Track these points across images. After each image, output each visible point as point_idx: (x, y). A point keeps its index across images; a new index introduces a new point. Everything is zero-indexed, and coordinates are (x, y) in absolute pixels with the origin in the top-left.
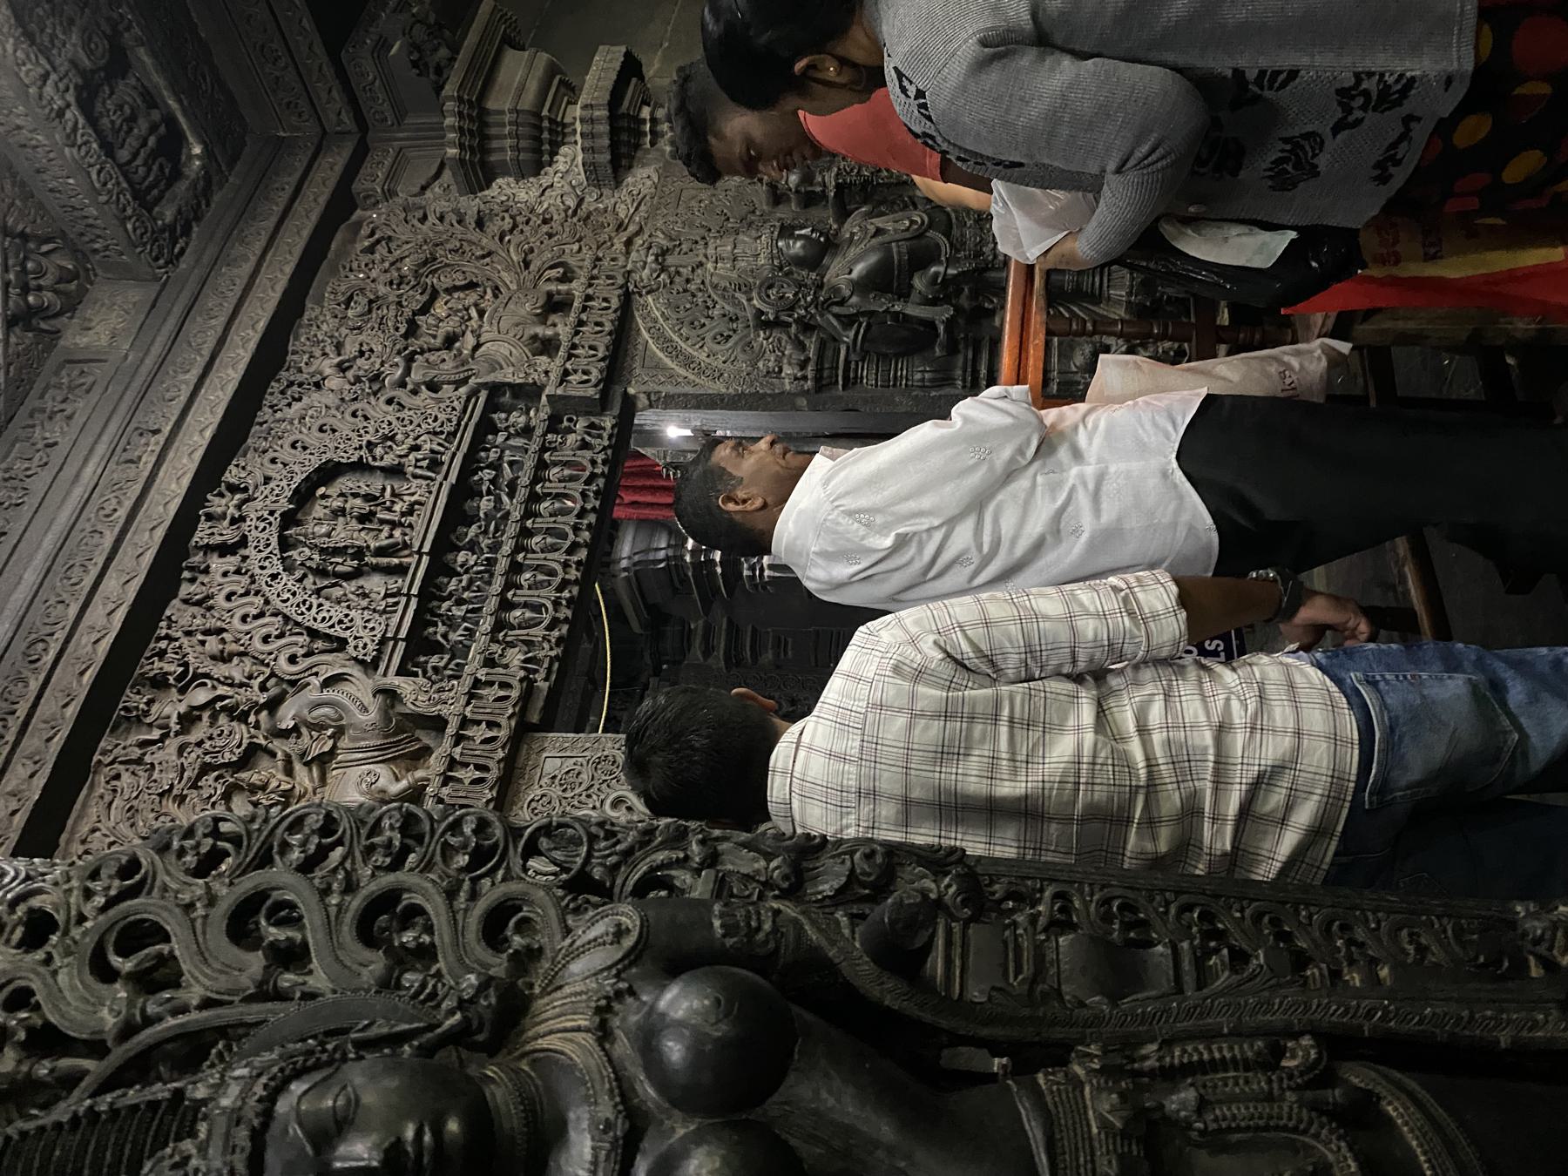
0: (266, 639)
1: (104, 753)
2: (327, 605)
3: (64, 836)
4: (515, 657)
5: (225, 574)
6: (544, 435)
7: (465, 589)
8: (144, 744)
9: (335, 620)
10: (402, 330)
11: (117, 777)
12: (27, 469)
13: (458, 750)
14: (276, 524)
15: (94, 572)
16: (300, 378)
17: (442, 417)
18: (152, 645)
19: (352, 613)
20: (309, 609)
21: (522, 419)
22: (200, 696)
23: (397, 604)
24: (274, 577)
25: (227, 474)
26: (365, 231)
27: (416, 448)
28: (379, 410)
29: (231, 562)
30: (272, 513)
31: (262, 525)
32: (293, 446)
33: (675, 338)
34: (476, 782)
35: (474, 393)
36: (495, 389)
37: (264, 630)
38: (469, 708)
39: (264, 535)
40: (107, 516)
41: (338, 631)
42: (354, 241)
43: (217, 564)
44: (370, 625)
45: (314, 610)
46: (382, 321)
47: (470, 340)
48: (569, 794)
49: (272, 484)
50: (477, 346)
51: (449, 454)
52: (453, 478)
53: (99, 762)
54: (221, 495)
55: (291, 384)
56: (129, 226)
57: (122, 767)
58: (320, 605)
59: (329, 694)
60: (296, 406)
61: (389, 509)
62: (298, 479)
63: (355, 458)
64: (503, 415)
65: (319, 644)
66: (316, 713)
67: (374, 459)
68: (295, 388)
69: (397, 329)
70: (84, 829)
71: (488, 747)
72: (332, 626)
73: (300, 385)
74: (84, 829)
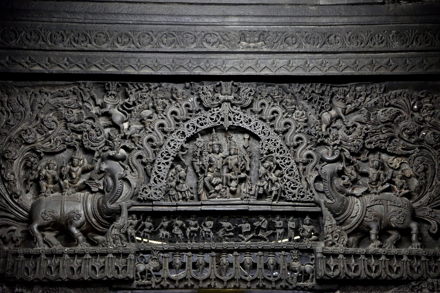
0: (150, 140)
1: (85, 84)
2: (168, 167)
3: (41, 83)
9: (159, 173)
10: (369, 146)
14: (216, 124)
15: (169, 49)
18: (144, 84)
19: (164, 181)
20: (165, 159)
23: (174, 199)
29: (196, 106)
30: (223, 120)
31: (214, 117)
32: (274, 112)
35: (318, 204)
39: (208, 120)
41: (153, 176)
43: (192, 99)
44: (158, 192)
50: (358, 197)
51: (270, 203)
53: (79, 84)
58: (167, 163)
62: (246, 126)
70: (46, 90)
72: (156, 173)
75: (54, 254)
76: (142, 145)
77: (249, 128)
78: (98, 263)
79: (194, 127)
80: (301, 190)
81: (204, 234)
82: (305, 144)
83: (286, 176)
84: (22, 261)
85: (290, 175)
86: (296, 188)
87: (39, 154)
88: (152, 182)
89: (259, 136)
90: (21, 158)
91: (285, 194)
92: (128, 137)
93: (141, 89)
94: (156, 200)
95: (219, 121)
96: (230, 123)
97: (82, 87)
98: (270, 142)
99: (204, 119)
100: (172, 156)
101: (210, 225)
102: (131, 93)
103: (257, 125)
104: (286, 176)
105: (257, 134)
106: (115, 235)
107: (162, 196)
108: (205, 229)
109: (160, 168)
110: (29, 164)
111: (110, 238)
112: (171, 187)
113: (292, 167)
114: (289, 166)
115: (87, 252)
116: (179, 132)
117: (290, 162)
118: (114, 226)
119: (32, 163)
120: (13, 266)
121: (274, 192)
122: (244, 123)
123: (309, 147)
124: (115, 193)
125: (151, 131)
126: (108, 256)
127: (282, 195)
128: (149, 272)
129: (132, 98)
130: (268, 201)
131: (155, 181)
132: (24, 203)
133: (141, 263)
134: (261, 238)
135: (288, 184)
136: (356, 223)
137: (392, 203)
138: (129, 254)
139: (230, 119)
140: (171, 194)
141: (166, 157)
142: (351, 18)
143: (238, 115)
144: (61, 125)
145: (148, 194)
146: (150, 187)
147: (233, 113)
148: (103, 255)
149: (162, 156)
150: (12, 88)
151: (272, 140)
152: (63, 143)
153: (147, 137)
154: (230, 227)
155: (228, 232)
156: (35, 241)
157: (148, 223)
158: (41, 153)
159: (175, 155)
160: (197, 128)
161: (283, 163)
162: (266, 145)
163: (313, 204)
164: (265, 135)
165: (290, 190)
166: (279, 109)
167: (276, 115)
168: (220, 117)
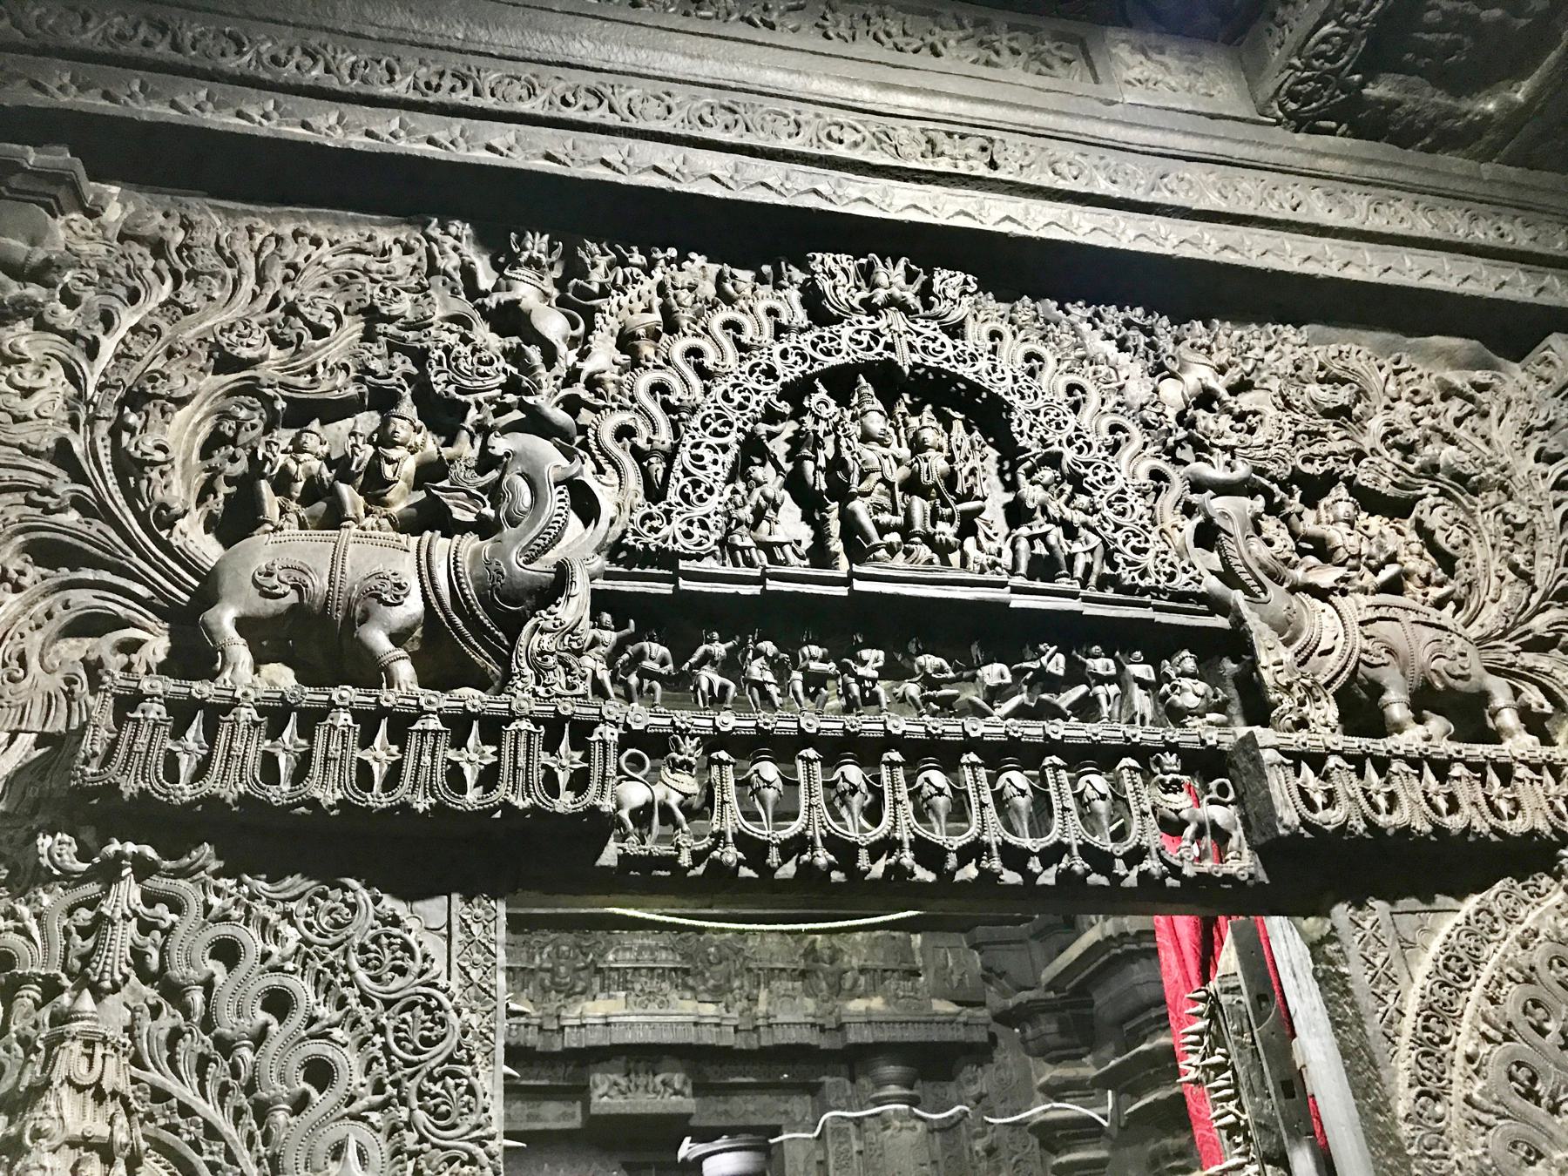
0: (659, 388)
2: (729, 458)
4: (677, 787)
5: (771, 312)
6: (1172, 748)
7: (805, 670)
8: (468, 272)
9: (700, 474)
10: (1308, 469)
11: (407, 251)
12: (889, 35)
13: (434, 723)
16: (1166, 343)
17: (1148, 560)
20: (716, 434)
21: (1189, 700)
22: (553, 325)
23: (750, 563)
24: (771, 373)
25: (946, 273)
26: (1480, 376)
27: (1071, 532)
28: (1134, 465)
29: (801, 317)
30: (890, 347)
33: (1487, 971)
34: (364, 769)
35: (1217, 605)
36: (1238, 643)
37: (675, 383)
38: (525, 725)
40: (829, 136)
42: (1456, 366)
44: (697, 531)
45: (714, 441)
46: (1315, 435)
47: (1326, 577)
48: (354, 960)
49: (944, 338)
52: (1018, 602)
54: (910, 278)
55: (1149, 332)
56: (1327, 29)
57: (423, 253)
58: (725, 448)
59: (556, 501)
60: (1110, 348)
61: (935, 517)
63: (1023, 442)
64: (1190, 664)
65: (658, 467)
66: (522, 484)
67: (1029, 473)
68: (1143, 339)
69: (1308, 460)
71: (439, 778)
72: (686, 473)
73: (1152, 345)
74: (320, 231)
75: (292, 708)
76: (633, 399)
77: (972, 377)
78: (474, 756)
79: (804, 357)
80: (1162, 556)
81: (855, 689)
82: (1137, 444)
83: (1108, 513)
84: (156, 725)
85: (1118, 513)
86: (1145, 551)
87: (268, 402)
88: (673, 496)
89: (1007, 398)
90: (206, 408)
91: (1114, 566)
92: (583, 376)
93: (623, 263)
94: (689, 557)
95: (879, 349)
96: (916, 358)
97: (435, 232)
98: (1041, 418)
99: (832, 340)
100: (739, 430)
101: (876, 661)
102: (594, 265)
103: (994, 370)
104: (1108, 513)
105: (1001, 393)
106: (542, 653)
107: (710, 545)
108: (861, 671)
109: (701, 458)
110: (228, 427)
111: (524, 664)
112: (739, 523)
113: (1123, 492)
114: (1112, 489)
115: (426, 707)
116: (758, 365)
117: (1113, 478)
118: (537, 625)
119: (239, 426)
120: (113, 745)
121: (1081, 556)
122: (953, 362)
123: (1151, 450)
124: (542, 523)
125: (661, 363)
126: (513, 726)
127: (1107, 570)
128: (666, 811)
129: (597, 278)
130: (1063, 584)
131: (685, 497)
132: (191, 547)
133: (631, 779)
134: (1055, 713)
135: (1120, 536)
136: (1344, 668)
137: (1423, 618)
138: (596, 724)
139: (912, 348)
140: (738, 541)
141: (721, 429)
142: (1209, 141)
143: (934, 340)
144: (354, 327)
145: (661, 534)
146: (668, 513)
147: (919, 334)
148: (493, 729)
149: (705, 426)
150: (202, 212)
151: (1046, 414)
152: (356, 380)
153: (645, 379)
154: (941, 670)
155: (937, 685)
156: (219, 665)
157: (655, 646)
158: (276, 398)
159: (748, 428)
160: (814, 360)
161: (1091, 479)
162: (1032, 427)
163: (1204, 607)
164: (1023, 398)
165: (1132, 556)
166: (1040, 349)
167: (1035, 363)
168: (882, 341)
